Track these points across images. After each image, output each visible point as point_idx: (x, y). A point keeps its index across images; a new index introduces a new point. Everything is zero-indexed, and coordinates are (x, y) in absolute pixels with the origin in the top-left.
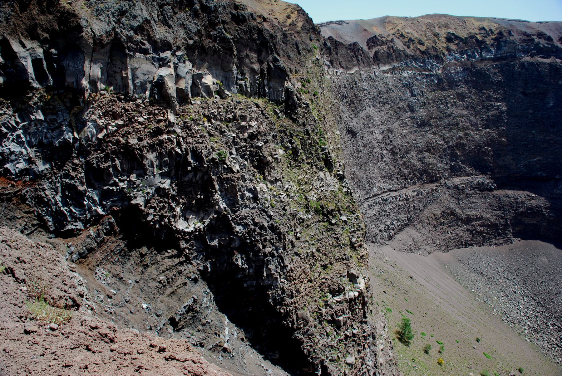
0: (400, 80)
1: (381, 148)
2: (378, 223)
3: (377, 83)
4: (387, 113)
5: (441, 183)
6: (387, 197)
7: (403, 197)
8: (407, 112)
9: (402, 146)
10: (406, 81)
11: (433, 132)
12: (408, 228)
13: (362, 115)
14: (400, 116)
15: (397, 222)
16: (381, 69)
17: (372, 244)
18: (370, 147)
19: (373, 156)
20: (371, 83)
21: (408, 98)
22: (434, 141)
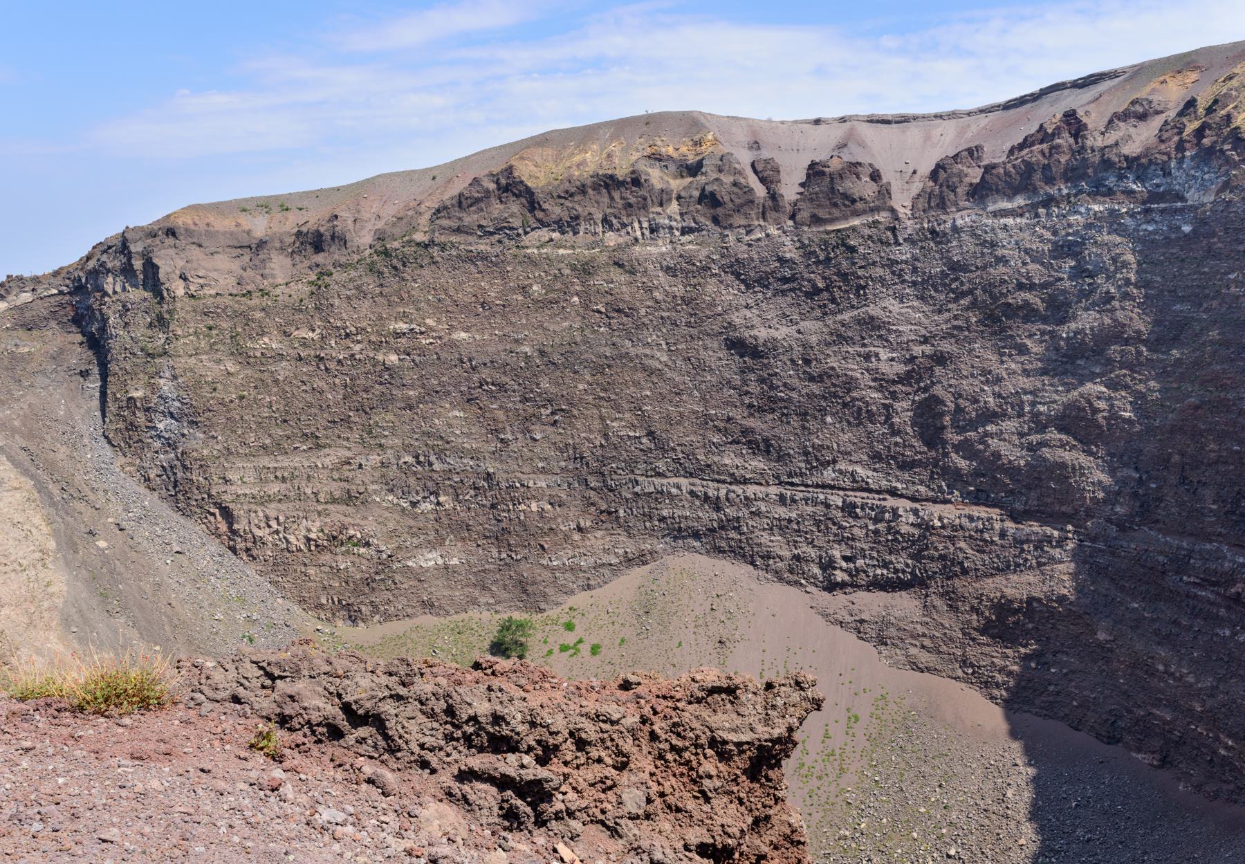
0: (1055, 233)
1: (894, 396)
2: (799, 539)
3: (955, 243)
4: (956, 317)
5: (1086, 528)
6: (859, 501)
7: (923, 519)
8: (1045, 320)
9: (976, 401)
10: (1068, 234)
11: (1111, 379)
12: (903, 593)
13: (846, 316)
14: (1003, 330)
15: (879, 566)
16: (990, 209)
17: (752, 567)
18: (835, 385)
19: (845, 405)
20: (932, 244)
21: (1061, 279)
22: (1102, 405)
